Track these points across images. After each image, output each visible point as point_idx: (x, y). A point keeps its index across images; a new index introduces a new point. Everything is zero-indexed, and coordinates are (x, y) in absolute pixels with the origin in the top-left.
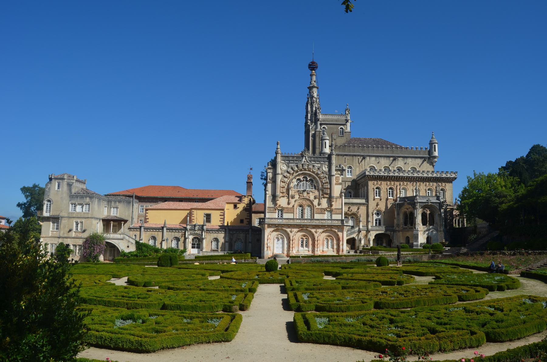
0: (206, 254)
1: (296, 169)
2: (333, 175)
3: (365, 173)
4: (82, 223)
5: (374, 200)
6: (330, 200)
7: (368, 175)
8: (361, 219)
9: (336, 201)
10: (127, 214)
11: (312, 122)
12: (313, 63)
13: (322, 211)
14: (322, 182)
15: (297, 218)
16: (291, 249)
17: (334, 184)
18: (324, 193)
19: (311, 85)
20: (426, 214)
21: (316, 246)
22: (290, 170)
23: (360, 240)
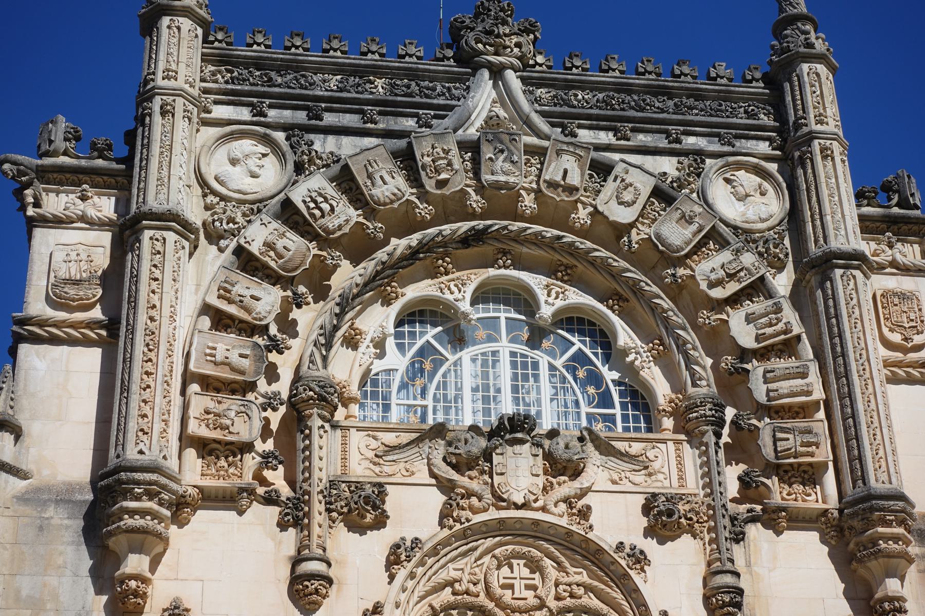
1: (390, 185)
14: (717, 339)
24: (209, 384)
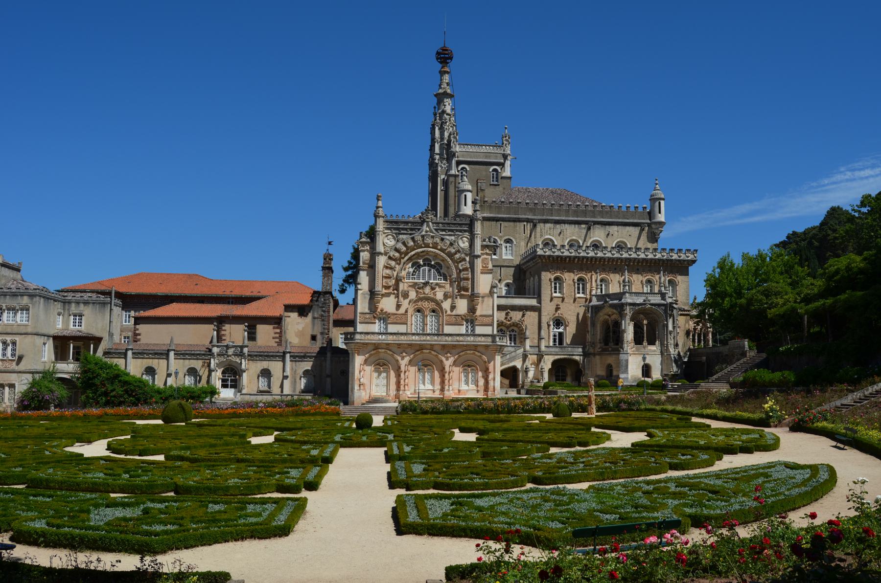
0: (247, 398)
1: (411, 243)
2: (478, 256)
3: (536, 251)
4: (14, 343)
5: (551, 300)
6: (473, 298)
7: (540, 256)
8: (528, 333)
9: (483, 301)
10: (100, 325)
11: (441, 158)
12: (444, 49)
13: (457, 320)
15: (414, 331)
16: (402, 387)
17: (479, 271)
18: (460, 289)
19: (441, 91)
20: (643, 325)
21: (446, 382)
22: (400, 246)
23: (526, 371)
24: (386, 277)
